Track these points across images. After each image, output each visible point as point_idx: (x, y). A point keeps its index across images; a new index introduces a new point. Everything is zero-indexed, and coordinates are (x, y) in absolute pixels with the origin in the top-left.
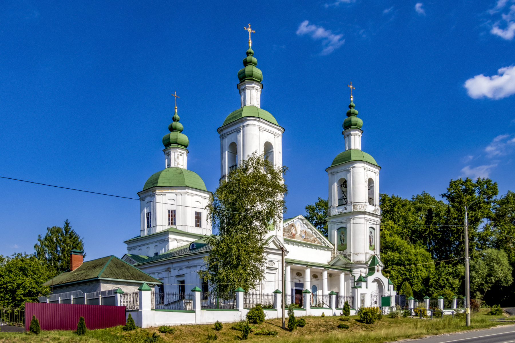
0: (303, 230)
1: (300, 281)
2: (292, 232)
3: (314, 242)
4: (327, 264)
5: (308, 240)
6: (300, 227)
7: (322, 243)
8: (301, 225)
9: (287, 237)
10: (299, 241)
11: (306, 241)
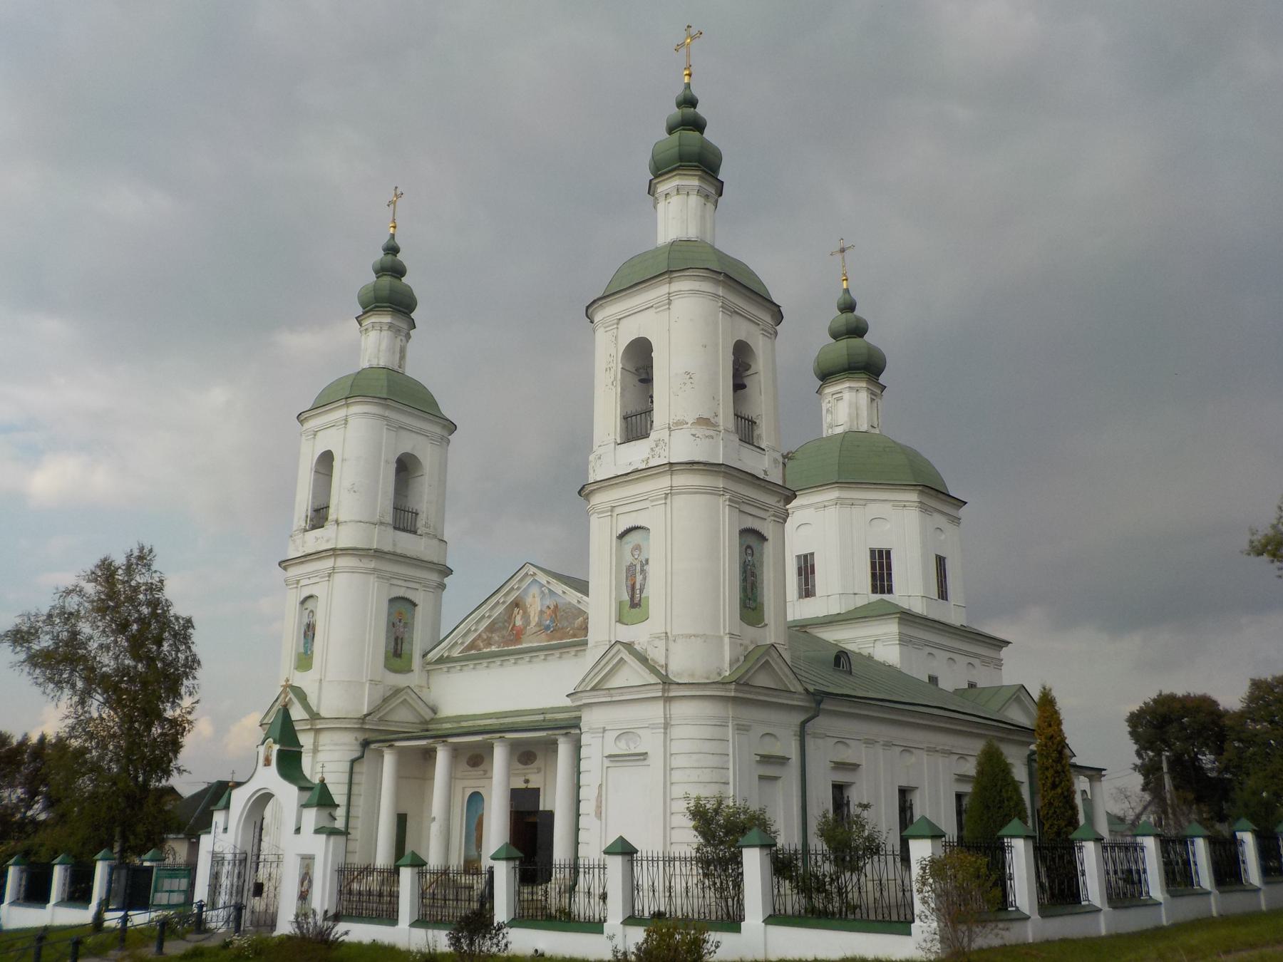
0: (548, 607)
1: (527, 781)
2: (514, 625)
6: (538, 599)
8: (542, 592)
10: (535, 645)
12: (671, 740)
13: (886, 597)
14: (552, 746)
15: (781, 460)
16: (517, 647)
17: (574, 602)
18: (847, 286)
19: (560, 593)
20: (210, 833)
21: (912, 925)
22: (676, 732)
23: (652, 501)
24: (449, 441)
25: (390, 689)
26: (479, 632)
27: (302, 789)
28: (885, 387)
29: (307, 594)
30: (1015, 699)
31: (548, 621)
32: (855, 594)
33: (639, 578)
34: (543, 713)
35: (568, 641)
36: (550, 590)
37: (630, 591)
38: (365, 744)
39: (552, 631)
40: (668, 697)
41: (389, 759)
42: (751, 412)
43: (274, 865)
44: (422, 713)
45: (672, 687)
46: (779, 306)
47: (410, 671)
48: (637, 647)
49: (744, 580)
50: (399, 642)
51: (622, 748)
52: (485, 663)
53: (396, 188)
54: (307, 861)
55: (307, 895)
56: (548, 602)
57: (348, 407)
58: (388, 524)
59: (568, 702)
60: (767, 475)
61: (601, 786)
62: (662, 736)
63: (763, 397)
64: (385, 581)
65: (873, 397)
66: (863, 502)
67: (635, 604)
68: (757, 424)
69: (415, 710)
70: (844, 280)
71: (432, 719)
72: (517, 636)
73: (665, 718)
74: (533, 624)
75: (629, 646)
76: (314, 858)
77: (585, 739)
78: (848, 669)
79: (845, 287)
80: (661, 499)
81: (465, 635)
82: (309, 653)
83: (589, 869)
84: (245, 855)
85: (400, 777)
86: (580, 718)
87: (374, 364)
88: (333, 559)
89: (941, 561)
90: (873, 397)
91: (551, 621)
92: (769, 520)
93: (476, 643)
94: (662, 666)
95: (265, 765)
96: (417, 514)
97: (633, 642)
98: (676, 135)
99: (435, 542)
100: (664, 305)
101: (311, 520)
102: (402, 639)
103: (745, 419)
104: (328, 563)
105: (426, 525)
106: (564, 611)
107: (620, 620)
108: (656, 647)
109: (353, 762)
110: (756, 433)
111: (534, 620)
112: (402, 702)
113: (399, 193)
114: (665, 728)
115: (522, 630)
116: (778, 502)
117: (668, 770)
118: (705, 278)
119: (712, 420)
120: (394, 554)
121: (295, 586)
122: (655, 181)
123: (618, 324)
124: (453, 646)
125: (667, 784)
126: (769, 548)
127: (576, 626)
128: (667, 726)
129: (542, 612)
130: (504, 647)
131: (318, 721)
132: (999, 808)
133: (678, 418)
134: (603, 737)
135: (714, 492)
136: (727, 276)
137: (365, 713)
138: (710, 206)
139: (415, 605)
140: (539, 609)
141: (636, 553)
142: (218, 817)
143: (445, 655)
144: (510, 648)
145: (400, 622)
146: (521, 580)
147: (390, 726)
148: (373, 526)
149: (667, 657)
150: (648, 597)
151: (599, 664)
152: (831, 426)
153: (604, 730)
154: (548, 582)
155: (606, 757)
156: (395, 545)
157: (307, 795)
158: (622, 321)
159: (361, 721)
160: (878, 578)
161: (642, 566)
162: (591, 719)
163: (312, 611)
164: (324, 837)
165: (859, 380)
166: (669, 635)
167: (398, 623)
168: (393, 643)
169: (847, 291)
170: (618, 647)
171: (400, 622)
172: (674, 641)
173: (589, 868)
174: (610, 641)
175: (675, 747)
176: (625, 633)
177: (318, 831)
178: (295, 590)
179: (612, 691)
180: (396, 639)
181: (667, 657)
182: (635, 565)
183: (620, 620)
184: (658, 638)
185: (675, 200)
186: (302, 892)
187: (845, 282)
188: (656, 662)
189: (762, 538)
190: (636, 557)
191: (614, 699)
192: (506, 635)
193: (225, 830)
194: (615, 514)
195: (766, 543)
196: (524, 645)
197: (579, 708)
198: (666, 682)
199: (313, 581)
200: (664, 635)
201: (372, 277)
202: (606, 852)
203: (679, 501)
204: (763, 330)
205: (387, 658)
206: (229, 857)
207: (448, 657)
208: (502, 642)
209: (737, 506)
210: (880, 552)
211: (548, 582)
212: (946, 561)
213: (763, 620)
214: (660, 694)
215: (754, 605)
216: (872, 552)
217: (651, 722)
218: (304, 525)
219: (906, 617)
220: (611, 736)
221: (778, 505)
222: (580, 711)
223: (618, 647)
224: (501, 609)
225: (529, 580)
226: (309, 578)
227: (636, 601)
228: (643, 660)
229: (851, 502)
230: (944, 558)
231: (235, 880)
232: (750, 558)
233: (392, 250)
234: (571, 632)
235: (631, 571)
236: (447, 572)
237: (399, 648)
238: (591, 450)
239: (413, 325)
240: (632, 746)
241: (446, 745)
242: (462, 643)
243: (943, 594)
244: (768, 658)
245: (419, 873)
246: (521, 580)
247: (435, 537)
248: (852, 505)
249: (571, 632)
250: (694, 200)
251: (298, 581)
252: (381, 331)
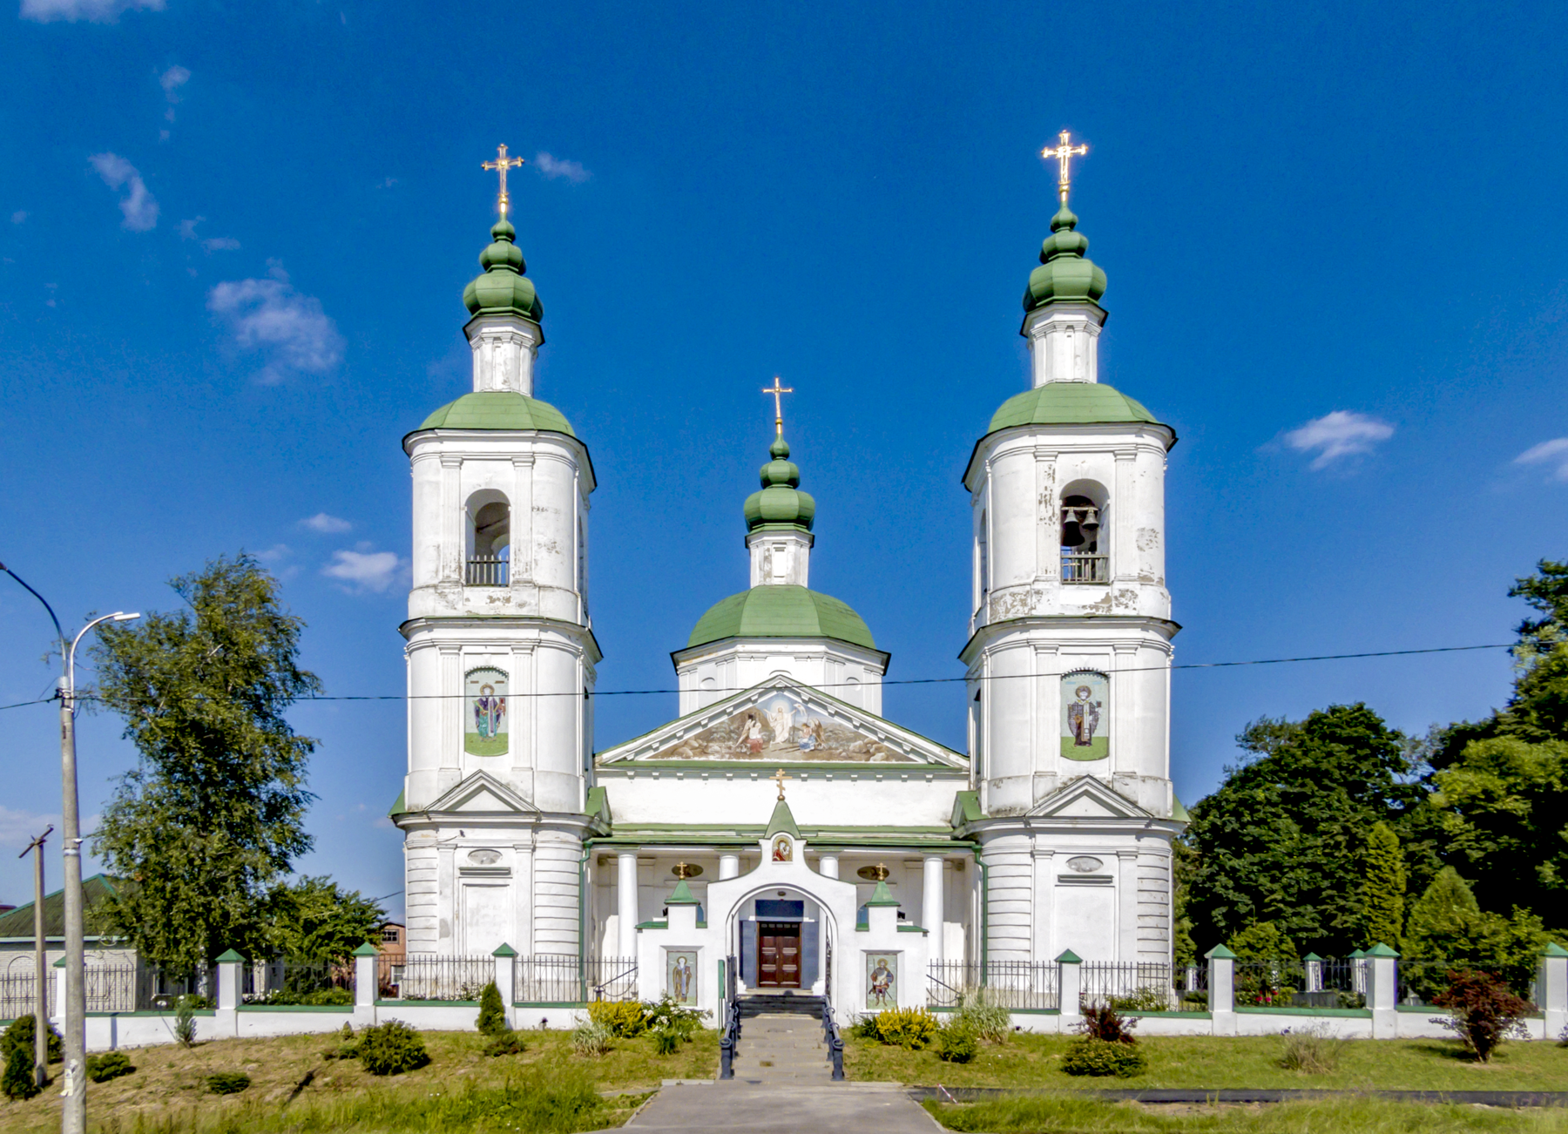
2: (747, 737)
3: (864, 756)
4: (943, 824)
5: (831, 754)
7: (911, 756)
8: (796, 708)
9: (723, 756)
11: (818, 758)
16: (753, 760)
33: (1087, 720)
37: (1075, 731)
67: (1079, 741)
81: (663, 742)
93: (681, 750)
111: (782, 735)
127: (851, 748)
140: (790, 725)
182: (1082, 706)
196: (766, 760)
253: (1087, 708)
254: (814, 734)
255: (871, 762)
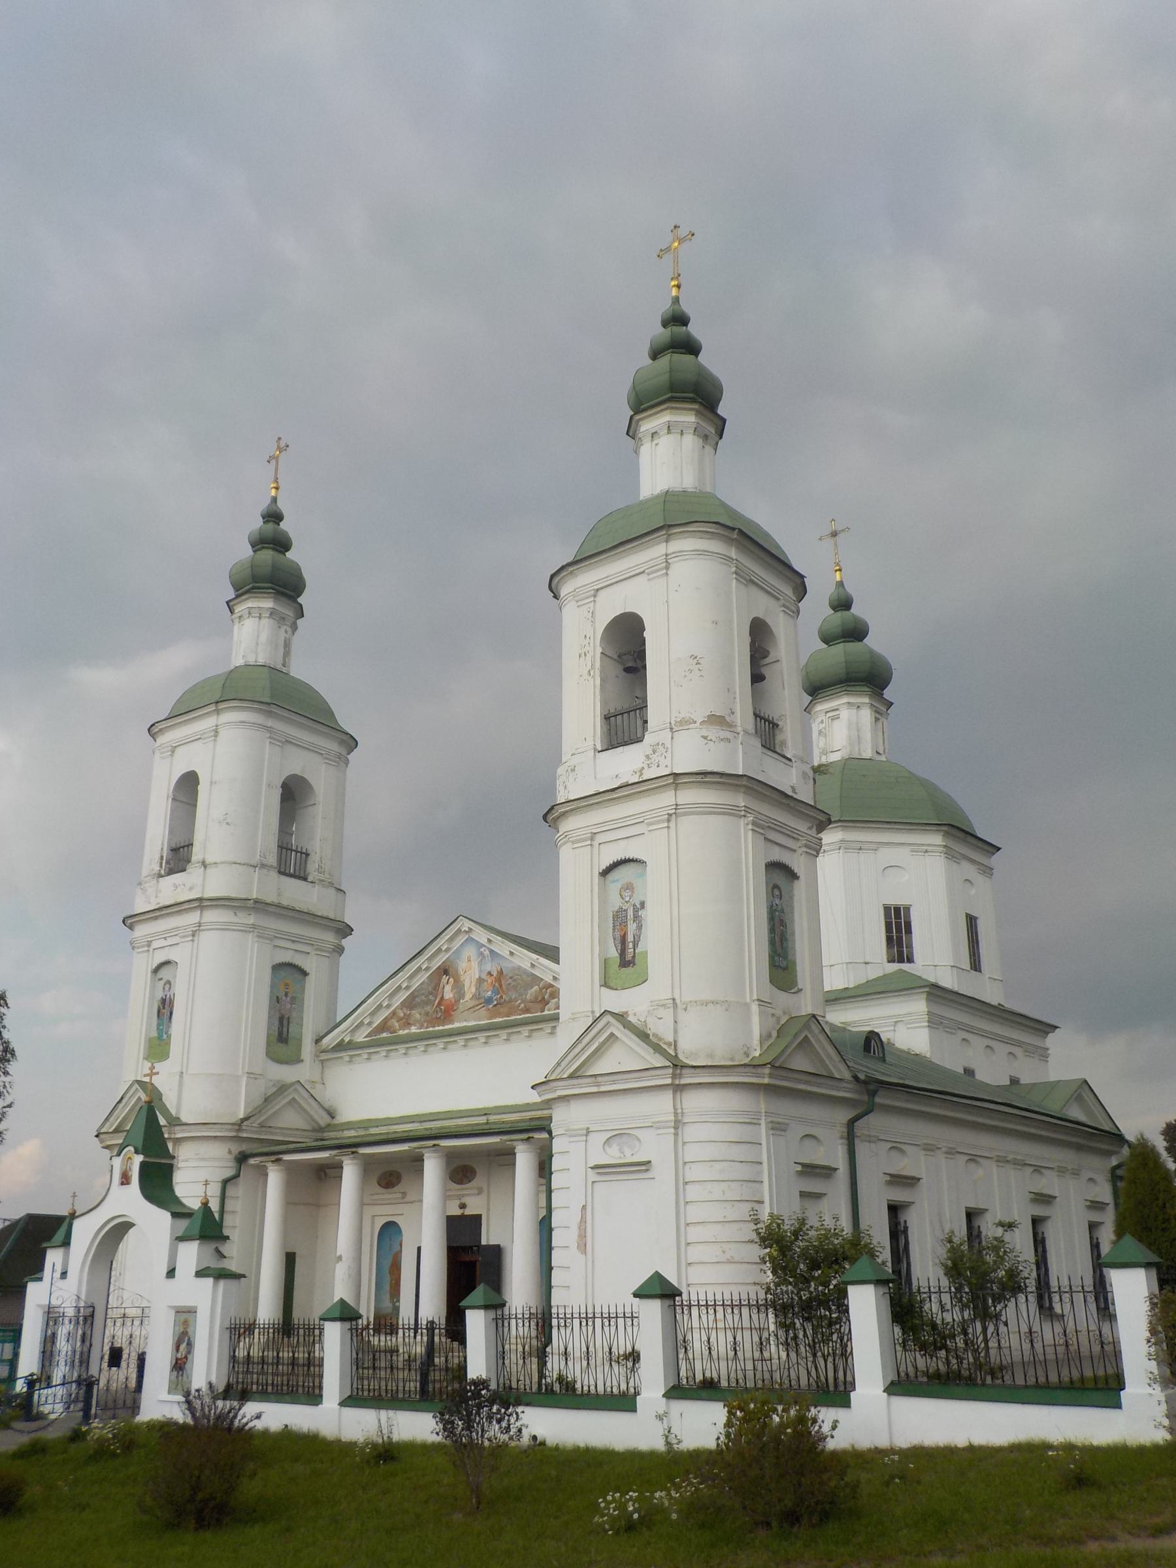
0: (490, 974)
1: (463, 1206)
2: (442, 998)
6: (475, 964)
8: (482, 954)
12: (684, 1143)
13: (905, 966)
14: (506, 1157)
15: (811, 773)
16: (447, 1027)
17: (526, 965)
18: (841, 577)
19: (506, 954)
20: (40, 1279)
21: (1122, 1392)
22: (690, 1133)
23: (649, 824)
24: (347, 762)
25: (274, 1085)
26: (392, 1009)
27: (175, 1215)
28: (892, 704)
29: (163, 959)
30: (1076, 1099)
31: (490, 993)
32: (866, 963)
33: (632, 927)
34: (485, 1114)
35: (519, 1017)
36: (491, 951)
38: (242, 1159)
39: (495, 1006)
40: (678, 1085)
41: (275, 1179)
42: (772, 713)
43: (137, 1322)
44: (316, 1117)
45: (685, 1071)
46: (802, 577)
47: (298, 1060)
48: (631, 1018)
49: (772, 930)
50: (285, 1022)
51: (612, 1155)
52: (401, 1049)
53: (279, 439)
54: (183, 1317)
55: (185, 1363)
56: (490, 966)
57: (218, 715)
58: (272, 866)
59: (534, 1097)
60: (796, 793)
61: (584, 1207)
62: (672, 1138)
63: (786, 692)
64: (269, 942)
65: (878, 716)
66: (874, 846)
67: (626, 962)
68: (780, 726)
69: (305, 1111)
70: (836, 571)
71: (329, 1125)
72: (447, 1012)
73: (676, 1114)
74: (468, 996)
75: (621, 1017)
76: (196, 1312)
77: (557, 1146)
78: (881, 1055)
79: (838, 579)
80: (662, 821)
81: (373, 1014)
82: (165, 1037)
83: (567, 1320)
84: (91, 1309)
85: (290, 1202)
86: (550, 1118)
87: (251, 660)
88: (199, 912)
89: (971, 921)
90: (878, 715)
91: (493, 992)
92: (800, 851)
93: (389, 1023)
94: (669, 1044)
95: (122, 1184)
96: (307, 855)
97: (627, 1013)
98: (665, 361)
99: (332, 891)
100: (662, 569)
101: (167, 862)
102: (289, 1018)
103: (766, 720)
104: (193, 918)
105: (320, 870)
106: (511, 978)
107: (605, 984)
108: (661, 1018)
109: (225, 1183)
110: (779, 738)
111: (470, 990)
112: (289, 1103)
113: (282, 444)
114: (676, 1128)
115: (453, 1005)
116: (810, 828)
117: (681, 1184)
118: (712, 536)
119: (728, 719)
120: (279, 906)
121: (146, 949)
122: (637, 417)
123: (595, 596)
124: (358, 1027)
125: (681, 1203)
126: (800, 888)
127: (528, 997)
128: (678, 1124)
129: (480, 981)
130: (427, 1027)
131: (177, 1128)
132: (1163, 1230)
133: (682, 716)
134: (586, 1141)
135: (733, 812)
136: (741, 532)
137: (241, 1116)
138: (709, 449)
139: (305, 974)
141: (627, 894)
142: (53, 1258)
143: (347, 1040)
144: (437, 1028)
145: (286, 995)
146: (451, 939)
147: (275, 1134)
148: (252, 869)
149: (676, 1031)
150: (647, 953)
151: (581, 1042)
152: (824, 752)
153: (588, 1132)
154: (490, 941)
155: (591, 1168)
156: (279, 895)
157: (183, 1224)
158: (601, 593)
159: (237, 1127)
160: (895, 942)
161: (636, 910)
162: (561, 1118)
163: (169, 982)
164: (209, 1281)
165: (860, 694)
166: (678, 1001)
167: (284, 997)
168: (277, 1023)
169: (840, 584)
170: (608, 1018)
171: (286, 995)
172: (685, 1009)
173: (587, 1318)
174: (593, 1012)
175: (691, 1153)
176: (615, 1001)
177: (200, 1274)
178: (146, 954)
179: (600, 1079)
180: (281, 1019)
181: (676, 1031)
182: (626, 911)
183: (605, 984)
184: (663, 1005)
185: (666, 442)
186: (177, 1359)
187: (838, 572)
188: (660, 1039)
189: (792, 875)
190: (627, 899)
191: (603, 1089)
192: (431, 1011)
193: (64, 1275)
194: (596, 843)
195: (796, 882)
196: (457, 1025)
197: (548, 1104)
198: (678, 1066)
199: (170, 941)
200: (671, 1001)
201: (248, 551)
202: (636, 1295)
203: (686, 824)
204: (784, 606)
205: (268, 1044)
206: (70, 1312)
207: (350, 1042)
208: (425, 1021)
209: (762, 831)
210: (897, 910)
211: (490, 941)
212: (978, 921)
213: (796, 984)
214: (669, 1081)
215: (785, 963)
216: (887, 909)
217: (656, 1120)
218: (158, 868)
219: (936, 992)
220: (597, 1140)
221: (809, 832)
222: (550, 1109)
223: (608, 1018)
224: (423, 977)
225: (462, 939)
226: (165, 938)
227: (629, 957)
228: (643, 1036)
229: (858, 846)
230: (976, 918)
231: (79, 1344)
232: (777, 901)
233: (273, 516)
234: (522, 1005)
235: (620, 918)
236: (345, 930)
237: (285, 1030)
238: (558, 761)
239: (301, 614)
240: (628, 1152)
241: (355, 1158)
242: (370, 1024)
243: (976, 965)
244: (806, 1033)
245: (351, 1329)
246: (451, 939)
247: (331, 884)
248: (860, 849)
249: (522, 1005)
250: (690, 441)
251: (149, 944)
252: (260, 618)
253: (630, 913)
254: (497, 985)
255: (546, 1012)
